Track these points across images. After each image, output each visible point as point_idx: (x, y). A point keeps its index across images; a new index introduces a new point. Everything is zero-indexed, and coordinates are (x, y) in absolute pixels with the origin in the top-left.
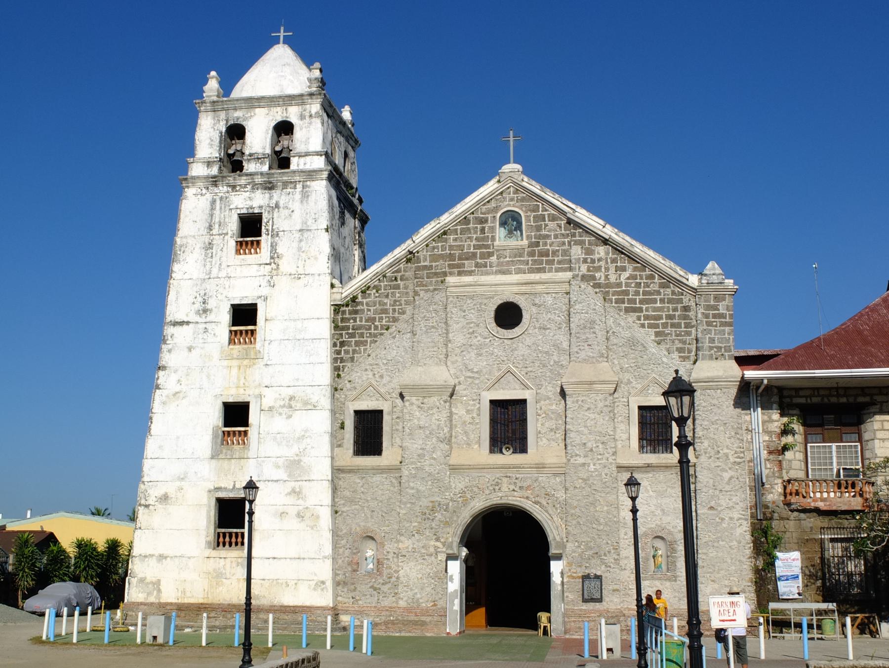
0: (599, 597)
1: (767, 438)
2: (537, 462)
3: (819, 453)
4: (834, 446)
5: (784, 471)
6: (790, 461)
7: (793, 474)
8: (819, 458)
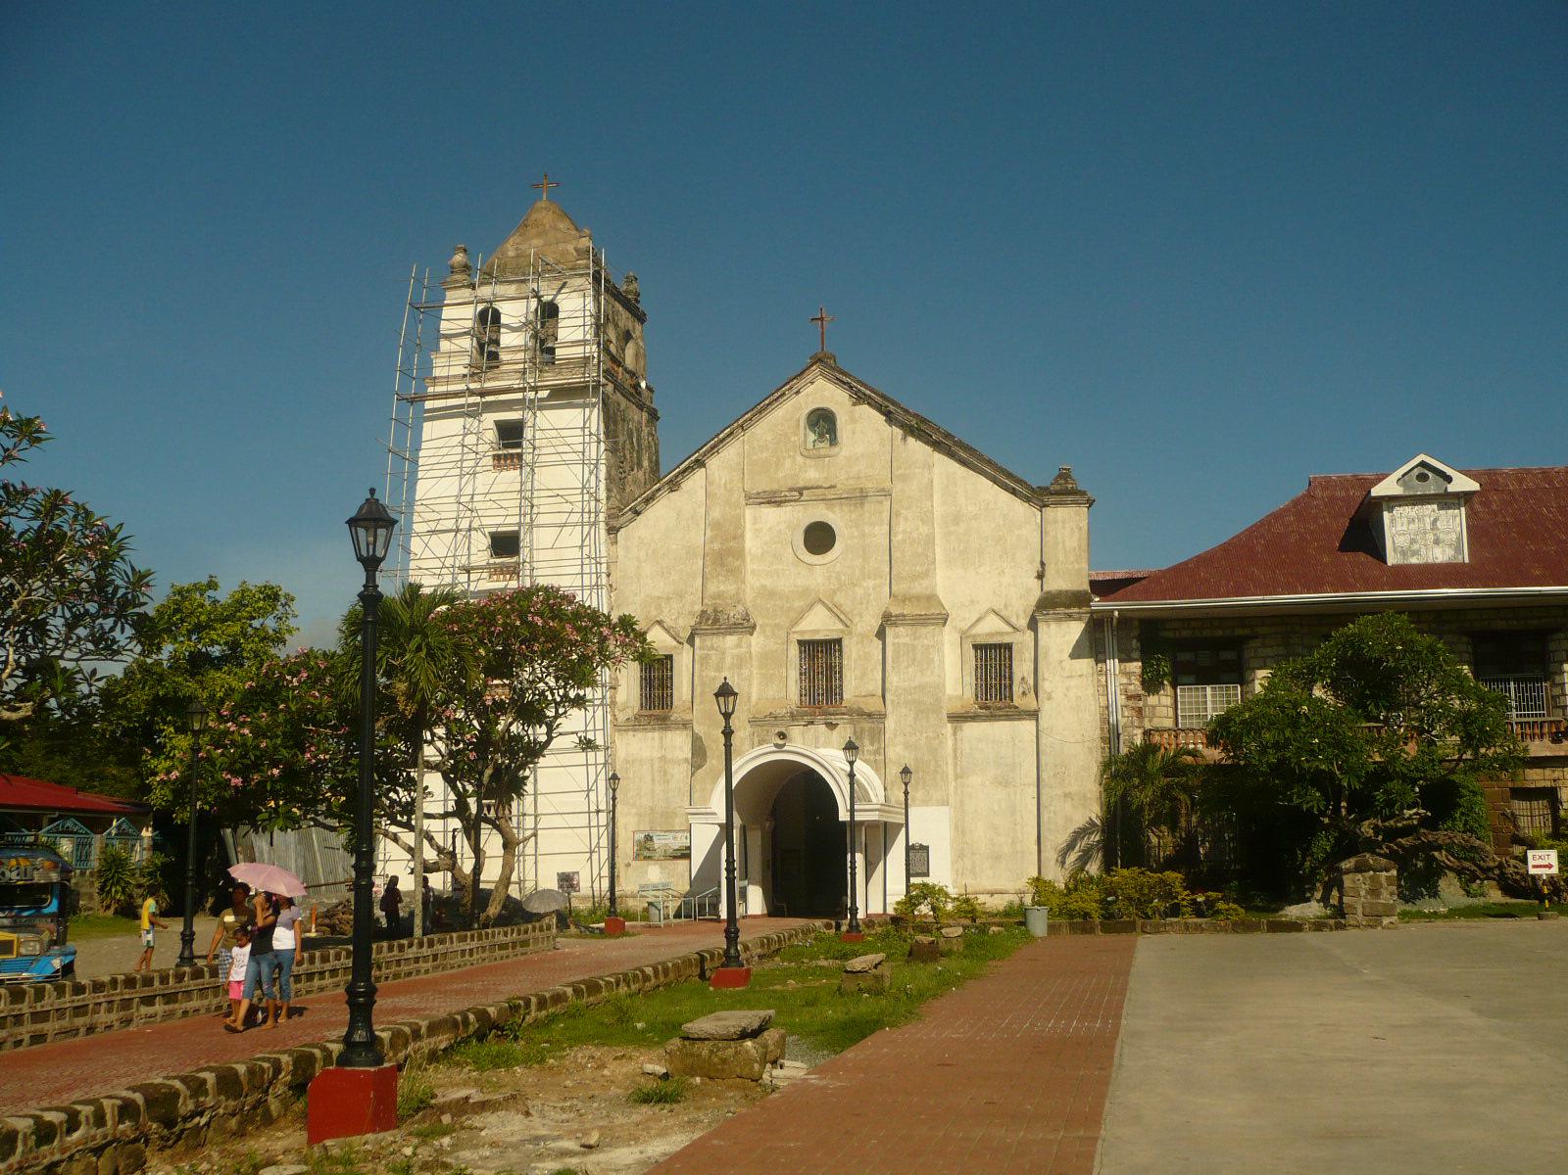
0: (926, 871)
1: (1125, 681)
2: (639, 688)
3: (1190, 697)
4: (1209, 689)
5: (1146, 720)
6: (1154, 707)
7: (1157, 723)
8: (1190, 703)
